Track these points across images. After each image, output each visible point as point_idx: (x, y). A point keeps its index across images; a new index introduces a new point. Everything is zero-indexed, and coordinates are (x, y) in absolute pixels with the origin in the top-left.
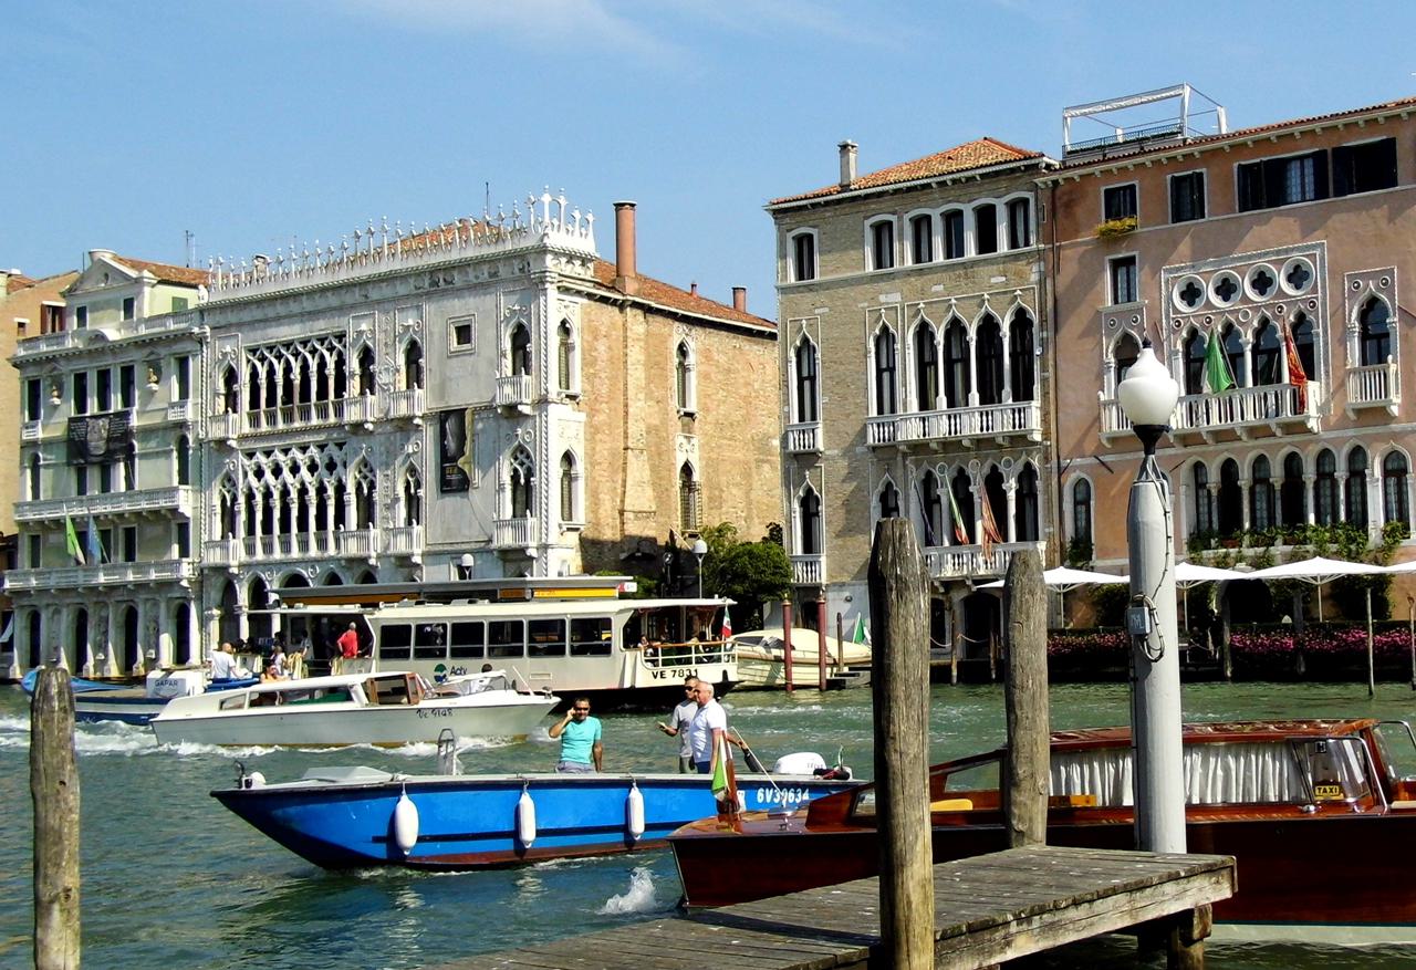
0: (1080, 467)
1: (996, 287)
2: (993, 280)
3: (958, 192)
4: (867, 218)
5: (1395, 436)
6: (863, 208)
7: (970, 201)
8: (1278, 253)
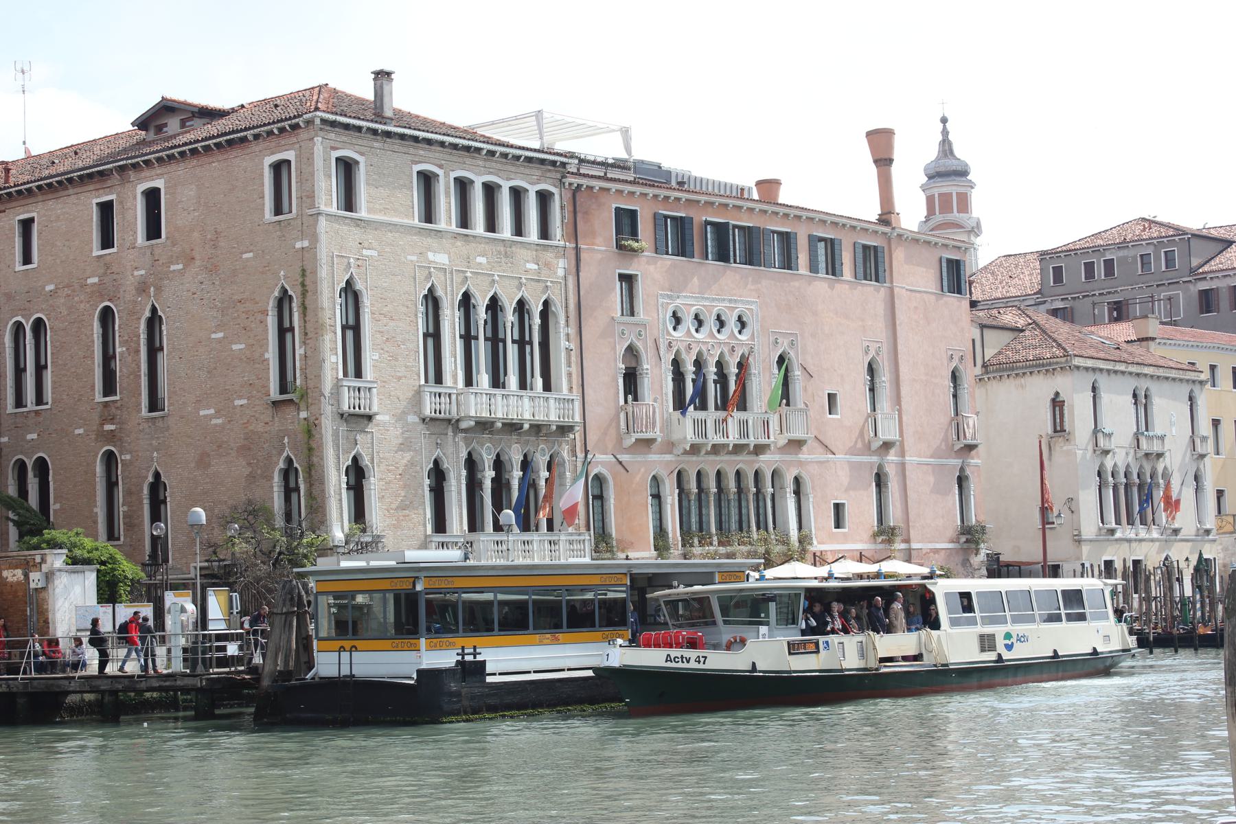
0: (602, 463)
1: (521, 270)
5: (801, 464)
6: (412, 151)
7: (508, 179)
8: (730, 301)
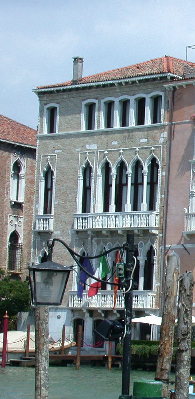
2: (142, 141)
3: (128, 89)
4: (84, 100)
7: (133, 95)
